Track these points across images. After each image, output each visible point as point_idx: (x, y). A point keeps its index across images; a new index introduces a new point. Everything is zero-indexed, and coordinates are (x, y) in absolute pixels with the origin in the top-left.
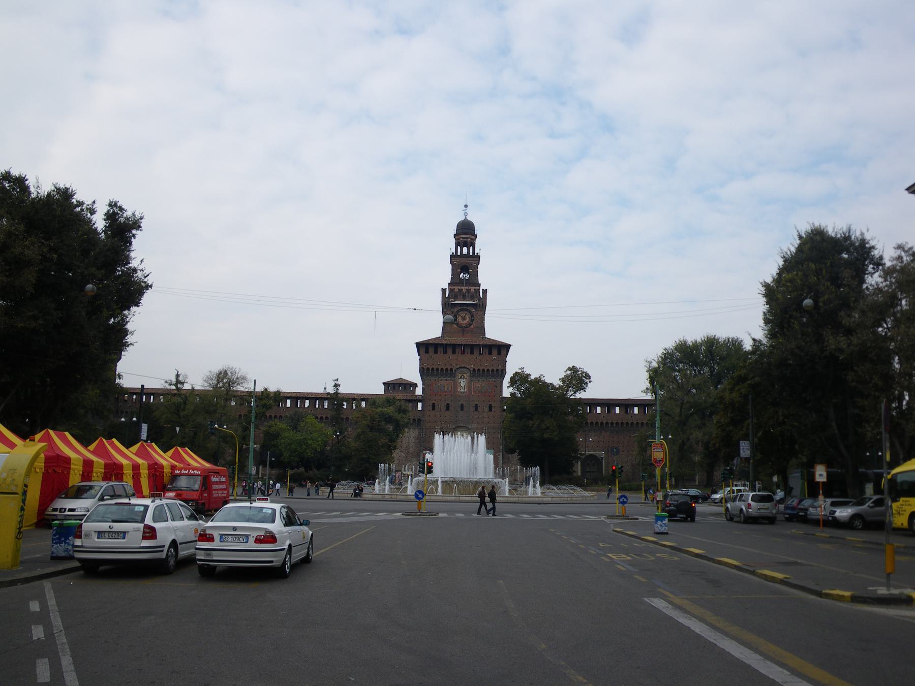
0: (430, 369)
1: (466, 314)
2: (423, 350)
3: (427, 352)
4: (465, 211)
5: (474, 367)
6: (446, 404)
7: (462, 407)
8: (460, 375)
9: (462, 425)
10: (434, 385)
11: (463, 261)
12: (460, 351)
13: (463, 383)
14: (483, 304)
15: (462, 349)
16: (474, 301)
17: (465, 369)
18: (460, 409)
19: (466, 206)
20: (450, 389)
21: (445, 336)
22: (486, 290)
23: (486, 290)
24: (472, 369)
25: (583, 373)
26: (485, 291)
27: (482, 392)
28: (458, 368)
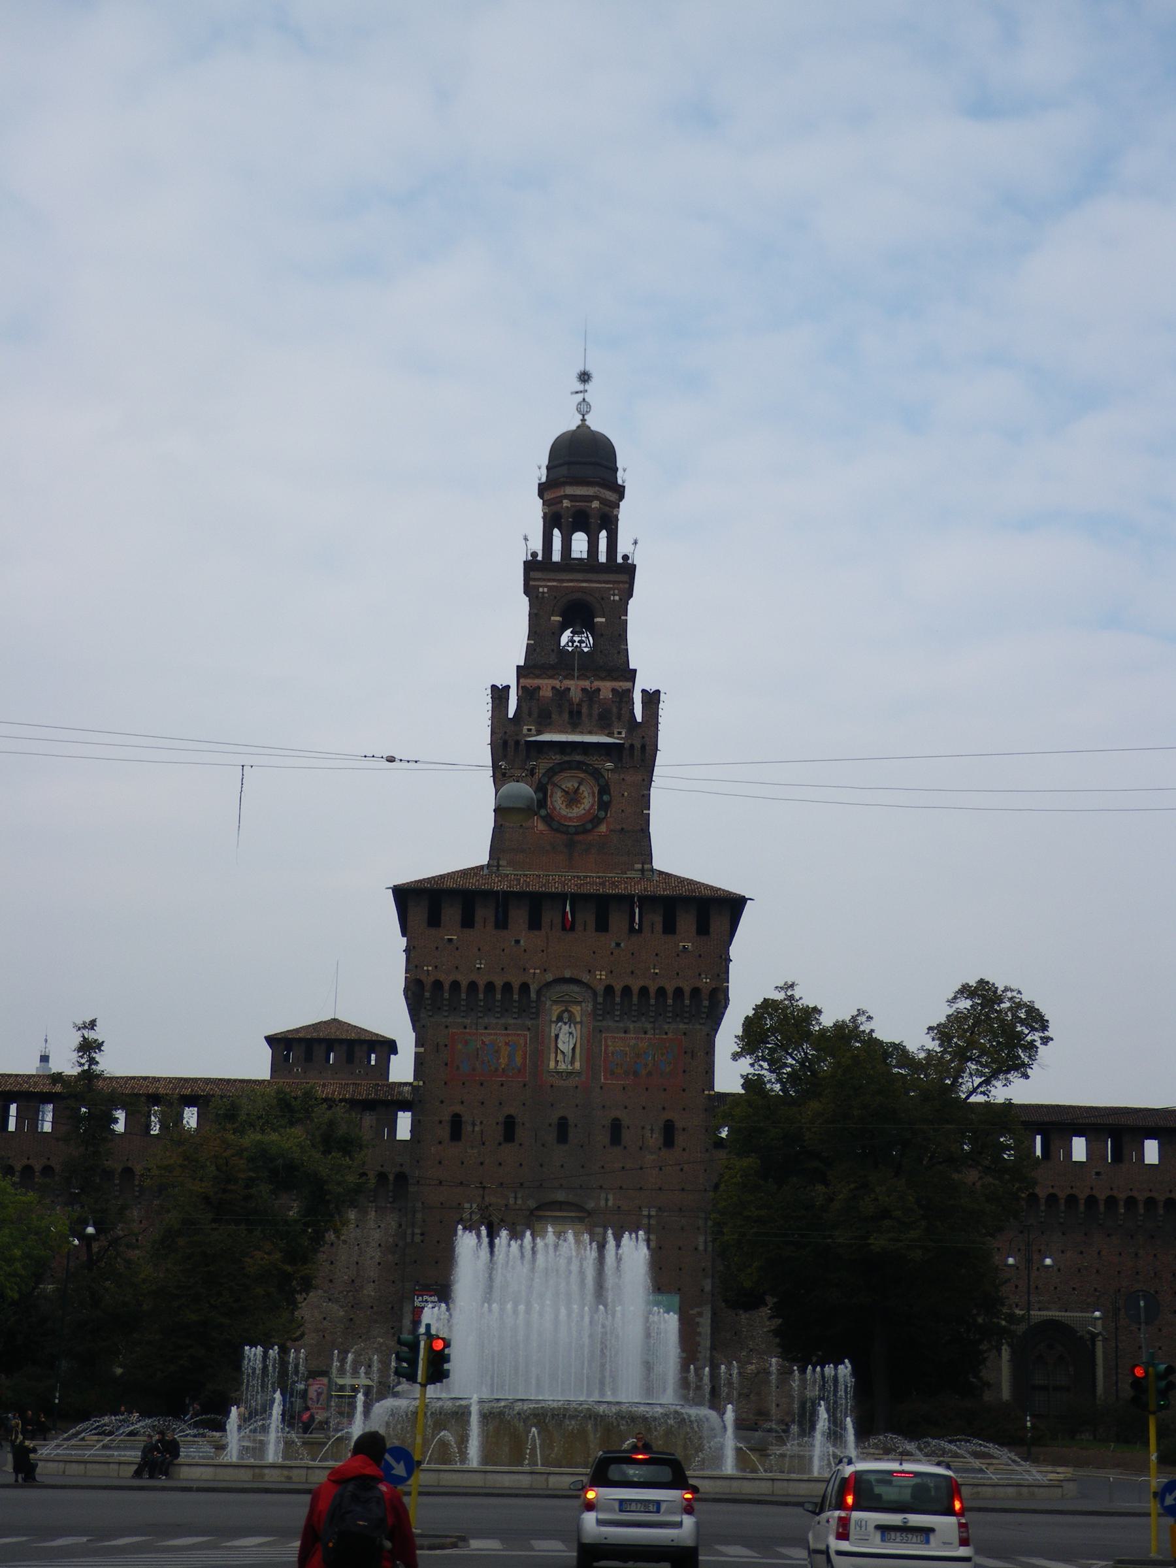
0: (447, 986)
1: (580, 784)
2: (419, 915)
3: (434, 921)
4: (580, 397)
5: (608, 982)
6: (501, 1119)
7: (562, 1129)
8: (556, 1010)
9: (561, 1196)
10: (460, 1046)
11: (571, 582)
12: (558, 920)
13: (567, 1038)
14: (643, 747)
15: (565, 913)
16: (610, 735)
17: (575, 988)
19: (585, 377)
20: (519, 1061)
21: (501, 863)
22: (658, 692)
23: (658, 692)
24: (600, 989)
25: (1019, 1005)
26: (652, 699)
27: (636, 1073)
28: (548, 985)
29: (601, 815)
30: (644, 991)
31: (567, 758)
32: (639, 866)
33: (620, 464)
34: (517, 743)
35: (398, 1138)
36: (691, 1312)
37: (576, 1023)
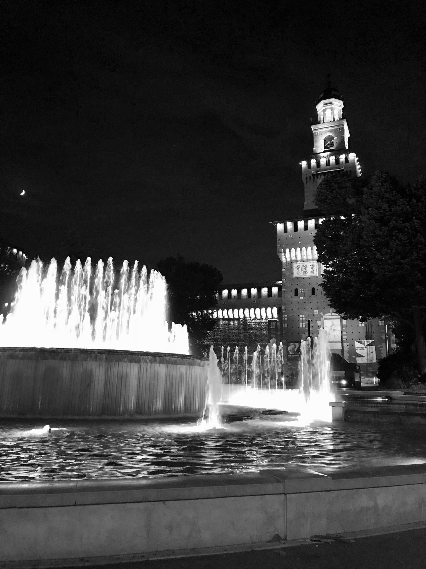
36: (378, 346)
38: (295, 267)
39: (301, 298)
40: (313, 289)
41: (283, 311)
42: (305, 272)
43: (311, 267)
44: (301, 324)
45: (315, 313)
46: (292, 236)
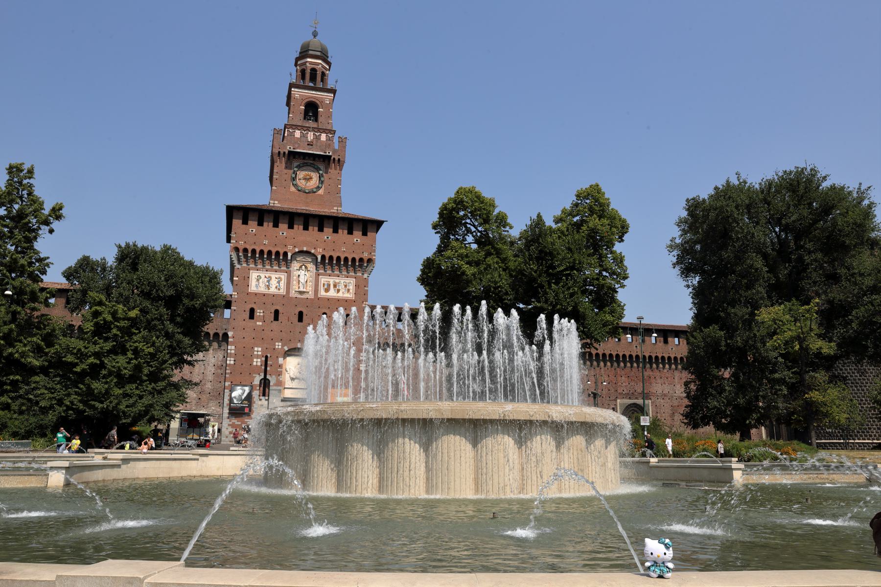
0: (250, 251)
6: (273, 311)
14: (339, 159)
18: (297, 319)
26: (342, 141)
29: (320, 185)
30: (339, 258)
31: (306, 161)
32: (336, 208)
33: (329, 55)
34: (284, 153)
35: (225, 317)
37: (308, 271)
38: (254, 277)
39: (258, 323)
40: (277, 313)
41: (230, 340)
42: (268, 287)
43: (277, 280)
44: (255, 360)
45: (277, 347)
46: (254, 232)
